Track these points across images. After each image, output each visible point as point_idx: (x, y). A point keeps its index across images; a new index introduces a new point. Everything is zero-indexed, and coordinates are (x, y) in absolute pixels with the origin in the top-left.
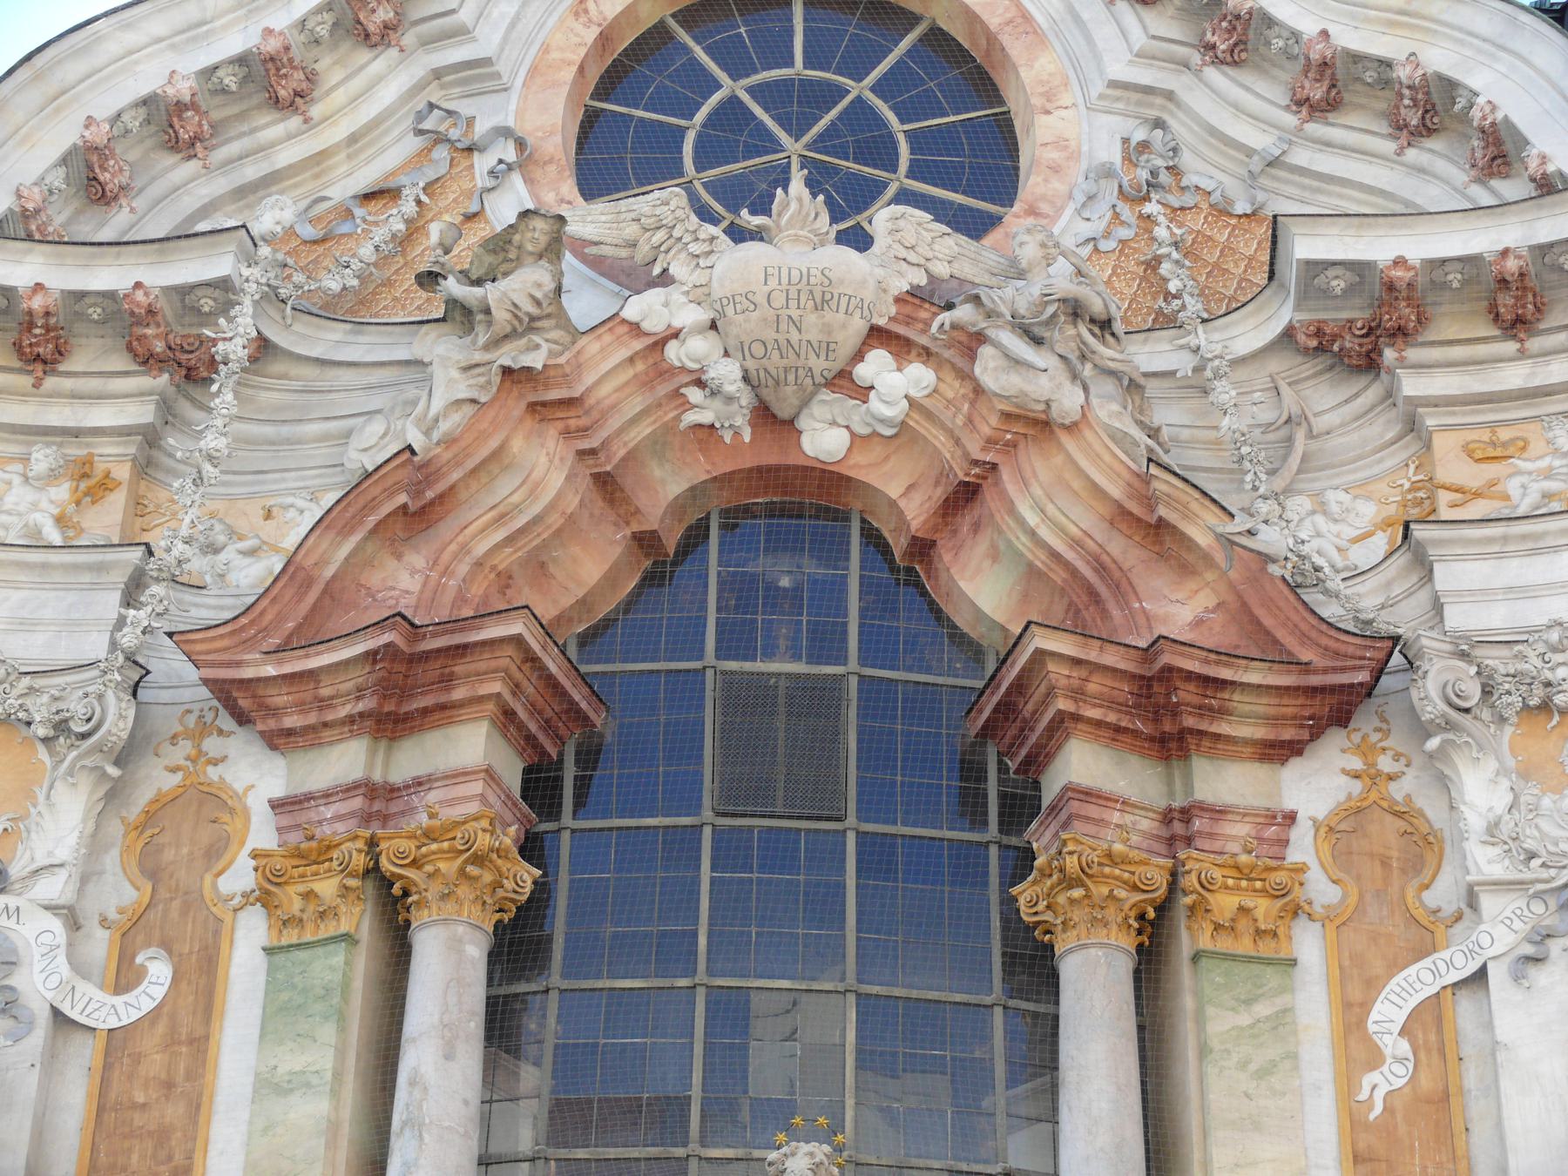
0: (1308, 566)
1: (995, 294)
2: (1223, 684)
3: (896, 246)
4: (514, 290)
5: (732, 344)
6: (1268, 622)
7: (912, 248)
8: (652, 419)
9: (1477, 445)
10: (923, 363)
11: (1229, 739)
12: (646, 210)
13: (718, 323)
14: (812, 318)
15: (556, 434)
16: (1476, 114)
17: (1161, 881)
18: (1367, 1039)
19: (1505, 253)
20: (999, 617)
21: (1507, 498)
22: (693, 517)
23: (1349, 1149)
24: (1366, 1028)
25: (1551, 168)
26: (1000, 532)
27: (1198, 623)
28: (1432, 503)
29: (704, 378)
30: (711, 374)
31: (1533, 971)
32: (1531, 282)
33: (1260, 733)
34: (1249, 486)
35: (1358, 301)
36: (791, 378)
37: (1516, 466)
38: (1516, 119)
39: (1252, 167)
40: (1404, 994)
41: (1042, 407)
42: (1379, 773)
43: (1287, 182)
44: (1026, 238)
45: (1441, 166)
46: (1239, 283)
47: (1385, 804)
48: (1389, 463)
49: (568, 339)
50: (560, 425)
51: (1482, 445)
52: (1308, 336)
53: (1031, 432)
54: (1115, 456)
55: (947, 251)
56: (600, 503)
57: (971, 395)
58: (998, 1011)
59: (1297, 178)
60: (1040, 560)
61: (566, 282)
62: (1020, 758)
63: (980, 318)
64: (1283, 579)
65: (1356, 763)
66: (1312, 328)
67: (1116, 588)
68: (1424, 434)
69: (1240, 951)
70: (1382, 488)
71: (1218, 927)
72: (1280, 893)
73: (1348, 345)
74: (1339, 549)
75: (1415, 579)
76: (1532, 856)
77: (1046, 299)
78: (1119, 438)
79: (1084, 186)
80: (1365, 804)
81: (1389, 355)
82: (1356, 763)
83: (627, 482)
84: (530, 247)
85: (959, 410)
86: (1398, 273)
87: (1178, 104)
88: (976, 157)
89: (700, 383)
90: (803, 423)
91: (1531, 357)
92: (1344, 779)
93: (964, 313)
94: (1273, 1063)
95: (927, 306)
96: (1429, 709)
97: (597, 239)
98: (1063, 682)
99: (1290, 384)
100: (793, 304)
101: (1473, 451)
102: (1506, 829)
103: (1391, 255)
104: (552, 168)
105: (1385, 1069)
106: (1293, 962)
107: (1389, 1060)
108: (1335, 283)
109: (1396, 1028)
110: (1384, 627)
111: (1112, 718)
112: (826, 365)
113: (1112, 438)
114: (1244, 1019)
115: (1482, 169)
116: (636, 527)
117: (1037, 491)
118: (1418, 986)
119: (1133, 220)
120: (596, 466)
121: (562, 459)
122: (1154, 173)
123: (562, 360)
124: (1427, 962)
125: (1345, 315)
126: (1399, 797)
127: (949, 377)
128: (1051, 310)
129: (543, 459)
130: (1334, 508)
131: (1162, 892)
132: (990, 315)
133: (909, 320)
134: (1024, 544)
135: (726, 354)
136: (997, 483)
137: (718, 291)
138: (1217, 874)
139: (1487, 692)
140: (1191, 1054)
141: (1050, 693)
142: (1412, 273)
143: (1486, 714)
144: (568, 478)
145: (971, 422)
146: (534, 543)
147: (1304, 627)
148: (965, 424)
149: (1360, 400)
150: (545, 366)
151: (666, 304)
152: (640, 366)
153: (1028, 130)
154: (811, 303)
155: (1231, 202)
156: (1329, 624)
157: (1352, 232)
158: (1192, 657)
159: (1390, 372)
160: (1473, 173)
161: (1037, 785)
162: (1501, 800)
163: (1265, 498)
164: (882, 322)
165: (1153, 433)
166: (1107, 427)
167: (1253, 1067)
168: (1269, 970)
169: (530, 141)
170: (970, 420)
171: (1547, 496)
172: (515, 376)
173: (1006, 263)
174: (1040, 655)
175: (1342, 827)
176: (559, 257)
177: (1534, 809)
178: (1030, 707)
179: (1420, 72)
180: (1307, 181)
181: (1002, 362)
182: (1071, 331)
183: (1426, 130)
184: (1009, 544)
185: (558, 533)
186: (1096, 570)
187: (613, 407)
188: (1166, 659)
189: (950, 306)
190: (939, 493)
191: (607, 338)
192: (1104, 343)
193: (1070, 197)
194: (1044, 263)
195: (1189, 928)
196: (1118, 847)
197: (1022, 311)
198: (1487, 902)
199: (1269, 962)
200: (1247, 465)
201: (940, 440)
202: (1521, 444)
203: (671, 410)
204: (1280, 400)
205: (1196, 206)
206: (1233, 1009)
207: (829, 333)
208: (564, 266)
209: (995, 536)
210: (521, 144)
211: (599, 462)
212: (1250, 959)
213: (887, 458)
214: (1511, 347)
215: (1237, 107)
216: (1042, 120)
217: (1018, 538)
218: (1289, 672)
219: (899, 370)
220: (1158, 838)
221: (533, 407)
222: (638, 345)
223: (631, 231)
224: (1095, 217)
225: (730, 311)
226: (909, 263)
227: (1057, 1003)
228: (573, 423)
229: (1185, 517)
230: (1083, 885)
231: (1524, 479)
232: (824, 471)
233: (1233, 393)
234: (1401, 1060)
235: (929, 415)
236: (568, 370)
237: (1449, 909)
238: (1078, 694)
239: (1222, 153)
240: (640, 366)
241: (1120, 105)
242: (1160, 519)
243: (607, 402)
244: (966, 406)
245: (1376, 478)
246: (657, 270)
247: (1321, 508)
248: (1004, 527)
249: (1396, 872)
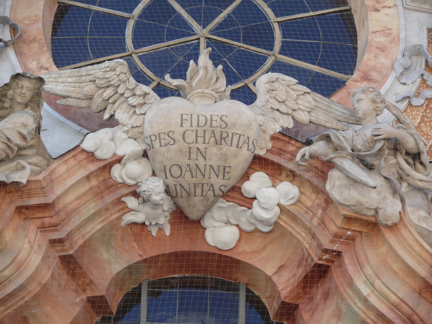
1: (340, 134)
3: (272, 101)
4: (8, 129)
5: (158, 166)
7: (283, 102)
8: (103, 218)
10: (290, 182)
12: (100, 74)
13: (149, 153)
14: (214, 150)
15: (36, 228)
22: (130, 286)
26: (343, 299)
29: (138, 190)
30: (143, 188)
36: (199, 191)
41: (372, 213)
44: (362, 96)
49: (45, 162)
50: (38, 222)
53: (365, 230)
55: (307, 105)
56: (65, 277)
57: (324, 204)
61: (44, 123)
63: (330, 151)
77: (375, 138)
79: (402, 61)
83: (84, 262)
84: (19, 99)
85: (315, 214)
88: (327, 40)
89: (135, 194)
90: (207, 222)
95: (293, 142)
97: (65, 94)
100: (200, 140)
104: (35, 45)
112: (223, 182)
113: (421, 235)
116: (90, 294)
117: (369, 271)
120: (63, 251)
121: (39, 246)
123: (40, 177)
127: (308, 191)
128: (379, 146)
129: (26, 246)
133: (281, 152)
134: (359, 308)
135: (154, 174)
136: (341, 265)
137: (148, 131)
144: (43, 259)
145: (323, 223)
146: (20, 304)
148: (319, 224)
150: (28, 181)
151: (112, 140)
152: (94, 182)
153: (364, 20)
154: (213, 139)
164: (262, 153)
166: (417, 227)
169: (20, 26)
170: (322, 221)
172: (8, 188)
173: (348, 113)
176: (39, 106)
181: (345, 181)
182: (392, 161)
184: (349, 307)
185: (36, 297)
187: (75, 210)
189: (309, 143)
190: (301, 272)
191: (72, 162)
192: (414, 166)
193: (392, 68)
194: (374, 114)
197: (359, 147)
203: (115, 213)
207: (225, 161)
208: (42, 113)
209: (339, 302)
210: (14, 29)
211: (65, 248)
213: (264, 248)
216: (373, 15)
217: (355, 304)
219: (274, 186)
221: (20, 210)
222: (93, 167)
223: (89, 88)
224: (409, 82)
225: (157, 144)
226: (281, 112)
228: (47, 221)
232: (220, 256)
235: (294, 218)
236: (44, 184)
240: (94, 182)
243: (71, 207)
244: (320, 212)
246: (106, 116)
248: (346, 296)
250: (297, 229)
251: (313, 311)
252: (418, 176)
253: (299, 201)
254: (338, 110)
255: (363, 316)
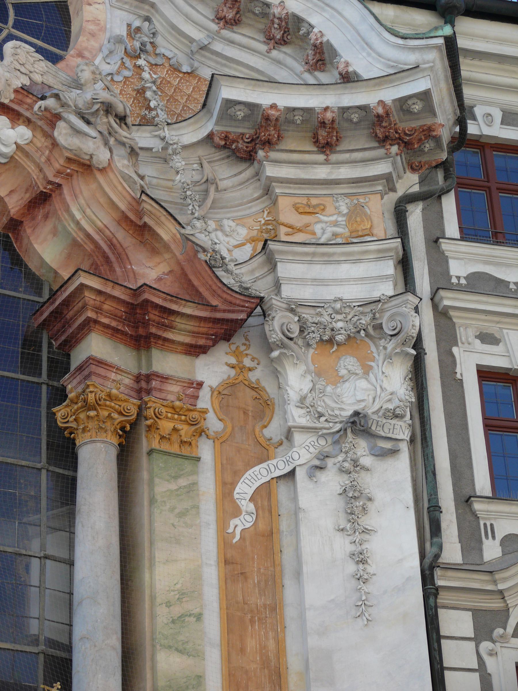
0: (218, 257)
1: (67, 95)
2: (172, 312)
3: (15, 62)
6: (196, 283)
7: (23, 65)
9: (301, 205)
10: (26, 126)
11: (172, 342)
16: (312, 36)
17: (134, 411)
18: (233, 501)
19: (326, 109)
20: (54, 266)
21: (314, 233)
23: (223, 556)
24: (233, 496)
25: (350, 69)
27: (159, 279)
28: (275, 233)
31: (318, 473)
32: (336, 126)
33: (187, 340)
34: (190, 212)
35: (247, 124)
37: (319, 218)
38: (336, 43)
39: (192, 49)
40: (252, 480)
41: (87, 157)
42: (244, 367)
43: (210, 59)
44: (85, 68)
45: (289, 61)
46: (183, 107)
47: (246, 383)
48: (254, 210)
51: (303, 206)
52: (221, 139)
53: (81, 170)
54: (124, 188)
55: (41, 69)
57: (50, 147)
58: (44, 472)
59: (214, 57)
60: (80, 237)
62: (59, 342)
63: (58, 106)
64: (206, 261)
65: (233, 360)
66: (223, 135)
67: (119, 257)
68: (273, 197)
69: (172, 451)
70: (250, 221)
71: (162, 437)
72: (193, 423)
73: (240, 146)
74: (228, 250)
75: (266, 270)
76: (321, 415)
77: (94, 101)
78: (127, 178)
79: (108, 46)
80: (237, 381)
81: (261, 153)
82: (233, 360)
86: (272, 112)
87: (157, 10)
88: (49, 22)
91: (330, 164)
92: (226, 368)
93: (50, 102)
94: (187, 510)
95: (31, 96)
96: (274, 336)
98: (92, 302)
99: (209, 162)
101: (298, 208)
102: (308, 402)
103: (270, 102)
105: (242, 517)
106: (198, 459)
107: (244, 513)
108: (238, 113)
109: (248, 497)
110: (254, 292)
111: (114, 324)
113: (123, 178)
114: (173, 486)
115: (312, 66)
118: (259, 476)
119: (131, 67)
122: (143, 44)
124: (264, 465)
125: (240, 130)
126: (253, 380)
127: (39, 135)
128: (96, 107)
130: (227, 229)
131: (134, 416)
132: (64, 105)
133: (20, 103)
134: (72, 229)
136: (61, 194)
138: (164, 410)
139: (301, 331)
140: (146, 503)
141: (84, 307)
142: (278, 113)
143: (300, 342)
145: (49, 160)
147: (214, 287)
148: (46, 162)
149: (243, 175)
153: (79, 11)
155: (180, 65)
156: (229, 288)
157: (250, 88)
158: (159, 297)
159: (260, 162)
160: (306, 67)
161: (69, 356)
162: (306, 386)
163: (198, 219)
165: (142, 178)
166: (121, 172)
167: (177, 511)
168: (186, 462)
170: (48, 160)
171: (335, 235)
173: (70, 79)
174: (82, 286)
175: (225, 392)
177: (323, 392)
178: (71, 313)
179: (285, 12)
180: (219, 60)
181: (69, 131)
182: (105, 120)
183: (283, 42)
184: (64, 227)
186: (110, 248)
188: (146, 296)
189: (43, 98)
190: (27, 196)
192: (120, 126)
193: (100, 50)
194: (93, 83)
195: (147, 437)
196: (114, 391)
197: (80, 106)
198: (298, 438)
199: (186, 458)
200: (188, 201)
201: (31, 168)
202: (322, 207)
204: (203, 171)
205: (162, 65)
206: (168, 481)
212: (177, 456)
214: (321, 157)
215: (187, 17)
216: (87, 8)
217: (69, 225)
218: (206, 310)
219: (13, 128)
220: (132, 389)
224: (112, 63)
226: (21, 72)
227: (75, 468)
229: (157, 223)
230: (96, 409)
231: (323, 225)
233: (183, 163)
234: (249, 514)
235: (27, 154)
237: (276, 439)
238: (98, 310)
239: (178, 40)
241: (127, 7)
242: (145, 223)
244: (47, 152)
245: (248, 216)
247: (220, 228)
248: (63, 218)
249: (250, 418)
250: (29, 163)
251: (34, 228)
252: (125, 134)
253: (31, 142)
254: (63, 76)
255: (74, 234)
